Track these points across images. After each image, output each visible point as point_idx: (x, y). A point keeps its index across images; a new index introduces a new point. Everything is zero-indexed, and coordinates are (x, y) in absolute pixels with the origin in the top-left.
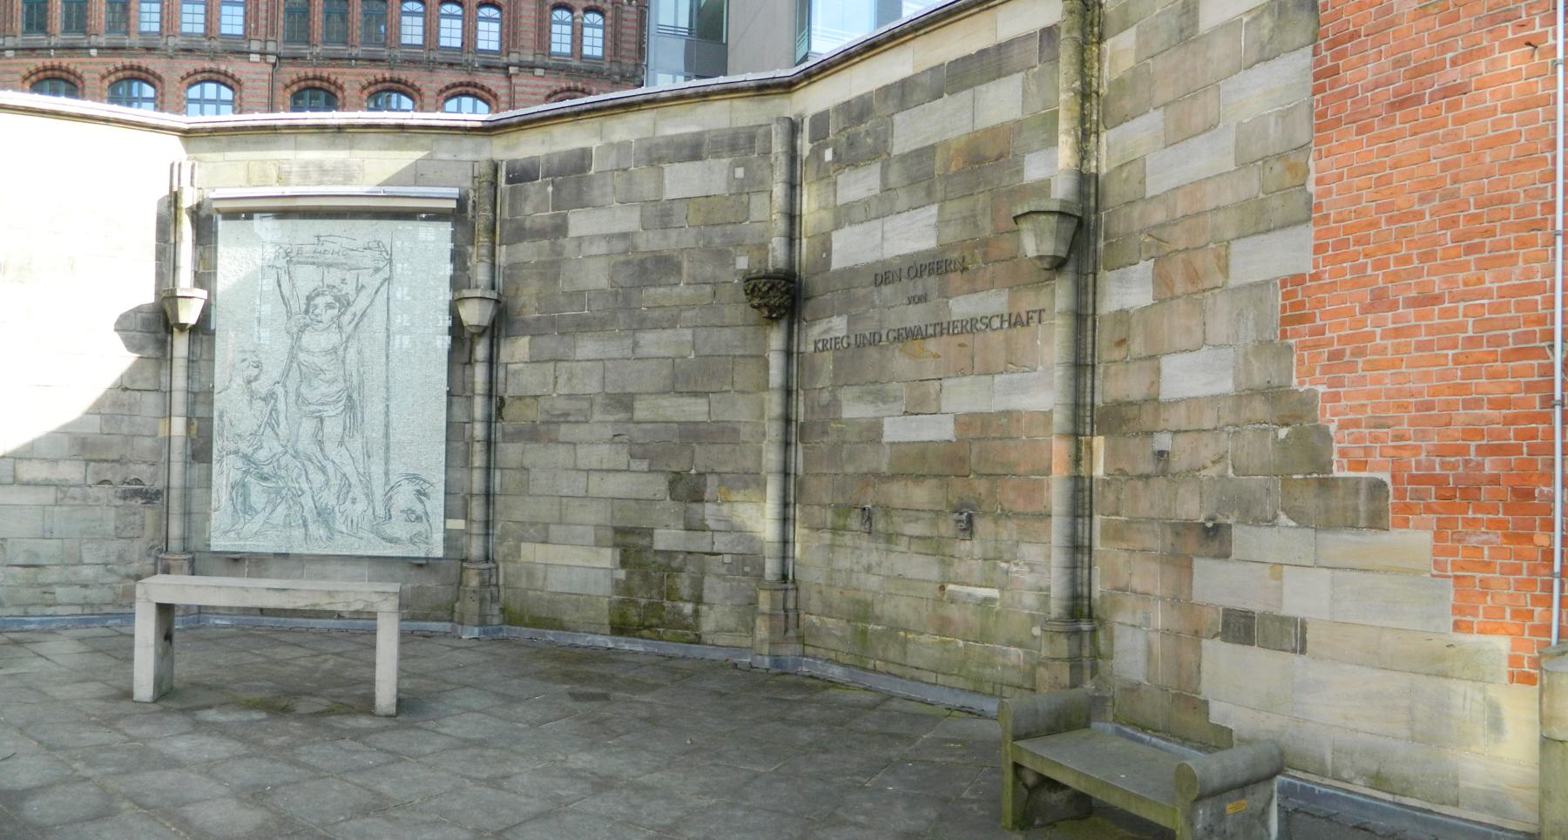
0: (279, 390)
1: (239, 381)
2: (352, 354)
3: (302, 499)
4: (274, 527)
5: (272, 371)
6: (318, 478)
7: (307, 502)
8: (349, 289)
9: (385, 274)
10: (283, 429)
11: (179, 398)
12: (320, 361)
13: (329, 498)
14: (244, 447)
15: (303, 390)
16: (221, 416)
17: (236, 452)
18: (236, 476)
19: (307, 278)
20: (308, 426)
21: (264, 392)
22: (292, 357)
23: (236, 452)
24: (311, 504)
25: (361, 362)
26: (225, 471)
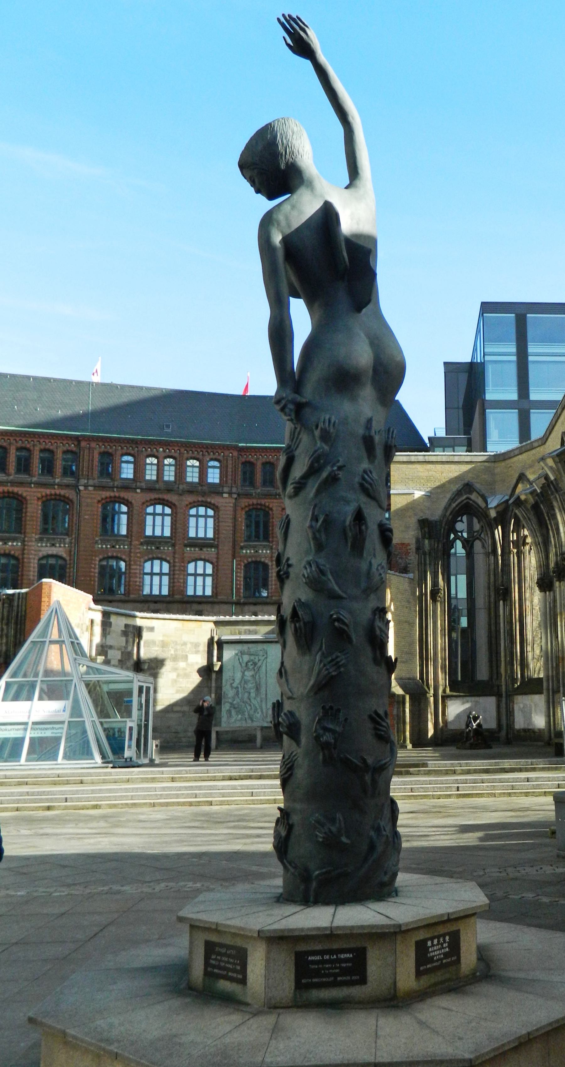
0: (239, 686)
2: (257, 677)
5: (237, 681)
6: (249, 708)
7: (246, 714)
8: (256, 660)
9: (265, 656)
10: (240, 695)
12: (249, 678)
13: (252, 712)
14: (230, 700)
15: (246, 686)
18: (228, 708)
19: (246, 658)
20: (246, 695)
22: (243, 677)
23: (228, 702)
25: (260, 678)
26: (225, 707)
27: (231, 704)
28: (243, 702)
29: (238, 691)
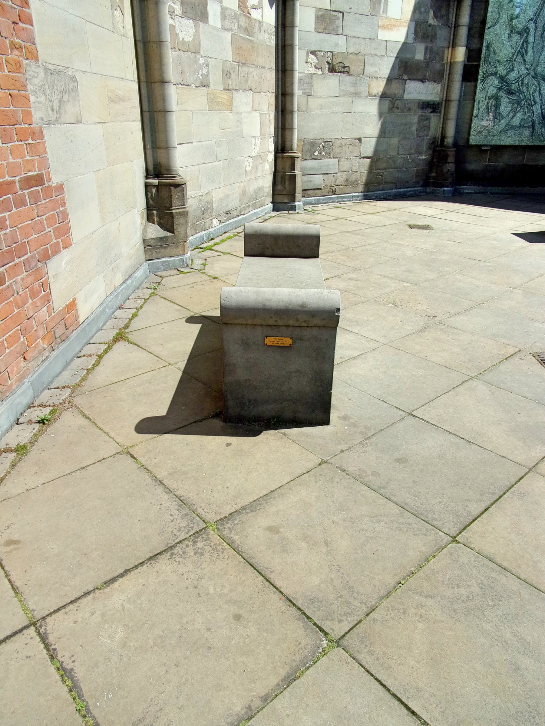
0: (532, 26)
1: (504, 17)
3: (534, 108)
4: (513, 127)
11: (463, 32)
14: (502, 71)
16: (488, 47)
17: (495, 74)
18: (492, 91)
21: (520, 26)
23: (495, 74)
24: (539, 111)
26: (486, 88)
27: (502, 79)
28: (535, 77)
29: (526, 41)
